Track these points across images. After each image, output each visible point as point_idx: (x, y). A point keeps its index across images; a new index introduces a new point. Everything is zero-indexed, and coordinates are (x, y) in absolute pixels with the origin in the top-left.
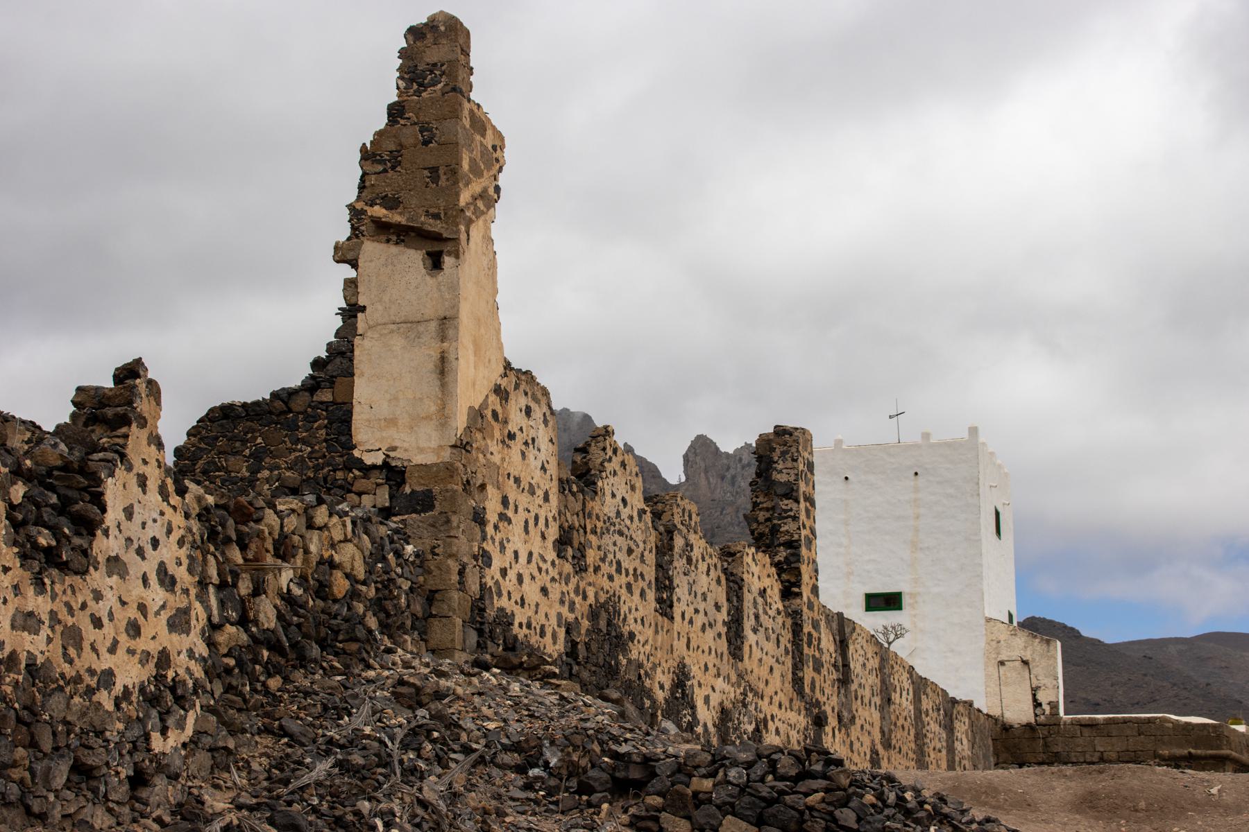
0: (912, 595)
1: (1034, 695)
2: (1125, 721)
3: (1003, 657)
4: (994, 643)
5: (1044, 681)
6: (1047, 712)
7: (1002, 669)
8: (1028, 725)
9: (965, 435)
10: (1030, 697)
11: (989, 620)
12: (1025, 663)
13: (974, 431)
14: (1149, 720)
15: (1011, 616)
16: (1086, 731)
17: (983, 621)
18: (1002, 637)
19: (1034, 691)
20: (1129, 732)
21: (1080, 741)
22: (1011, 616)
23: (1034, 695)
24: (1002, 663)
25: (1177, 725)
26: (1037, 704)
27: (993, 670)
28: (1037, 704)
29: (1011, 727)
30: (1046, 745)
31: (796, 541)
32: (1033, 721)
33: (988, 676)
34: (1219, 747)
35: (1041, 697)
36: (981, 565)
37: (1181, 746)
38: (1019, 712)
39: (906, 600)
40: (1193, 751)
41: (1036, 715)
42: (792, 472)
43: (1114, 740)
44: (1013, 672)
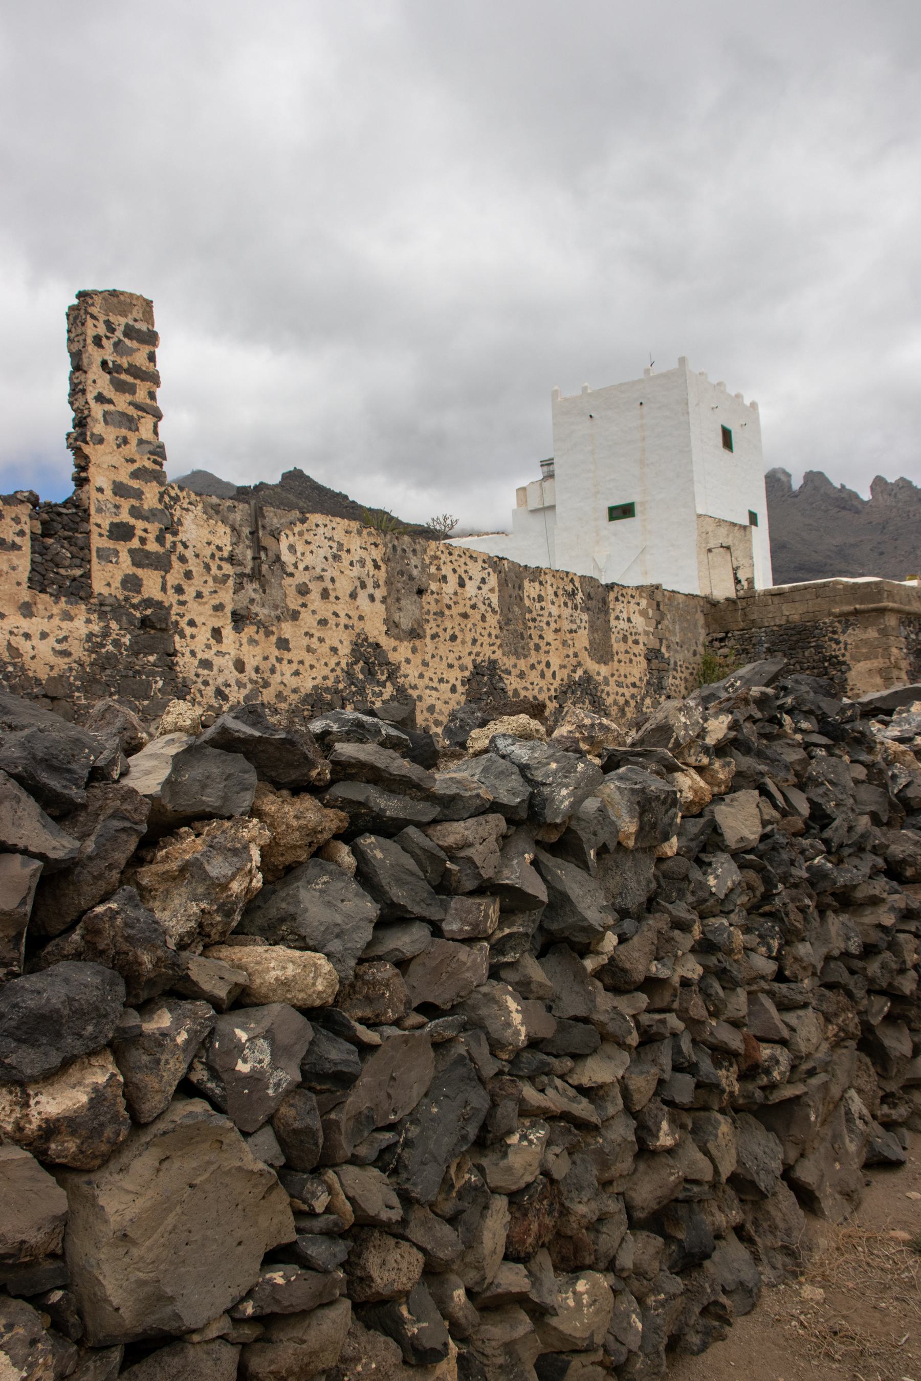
0: (643, 504)
1: (735, 574)
2: (806, 588)
3: (711, 546)
4: (704, 535)
5: (743, 561)
6: (746, 587)
7: (710, 555)
8: (727, 599)
9: (675, 365)
10: (732, 576)
11: (699, 516)
12: (728, 548)
13: (682, 361)
14: (825, 585)
15: (753, 518)
16: (776, 600)
17: (695, 518)
18: (710, 529)
19: (735, 570)
20: (808, 597)
21: (771, 608)
22: (753, 518)
23: (735, 574)
24: (710, 550)
25: (846, 585)
26: (738, 581)
27: (703, 557)
28: (738, 581)
29: (718, 602)
30: (745, 615)
31: (85, 418)
32: (732, 594)
33: (700, 563)
34: (880, 601)
35: (742, 575)
36: (692, 471)
37: (850, 604)
38: (723, 590)
39: (638, 509)
40: (858, 606)
41: (737, 591)
42: (81, 338)
43: (797, 605)
44: (719, 556)
